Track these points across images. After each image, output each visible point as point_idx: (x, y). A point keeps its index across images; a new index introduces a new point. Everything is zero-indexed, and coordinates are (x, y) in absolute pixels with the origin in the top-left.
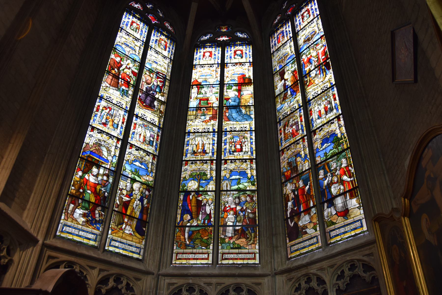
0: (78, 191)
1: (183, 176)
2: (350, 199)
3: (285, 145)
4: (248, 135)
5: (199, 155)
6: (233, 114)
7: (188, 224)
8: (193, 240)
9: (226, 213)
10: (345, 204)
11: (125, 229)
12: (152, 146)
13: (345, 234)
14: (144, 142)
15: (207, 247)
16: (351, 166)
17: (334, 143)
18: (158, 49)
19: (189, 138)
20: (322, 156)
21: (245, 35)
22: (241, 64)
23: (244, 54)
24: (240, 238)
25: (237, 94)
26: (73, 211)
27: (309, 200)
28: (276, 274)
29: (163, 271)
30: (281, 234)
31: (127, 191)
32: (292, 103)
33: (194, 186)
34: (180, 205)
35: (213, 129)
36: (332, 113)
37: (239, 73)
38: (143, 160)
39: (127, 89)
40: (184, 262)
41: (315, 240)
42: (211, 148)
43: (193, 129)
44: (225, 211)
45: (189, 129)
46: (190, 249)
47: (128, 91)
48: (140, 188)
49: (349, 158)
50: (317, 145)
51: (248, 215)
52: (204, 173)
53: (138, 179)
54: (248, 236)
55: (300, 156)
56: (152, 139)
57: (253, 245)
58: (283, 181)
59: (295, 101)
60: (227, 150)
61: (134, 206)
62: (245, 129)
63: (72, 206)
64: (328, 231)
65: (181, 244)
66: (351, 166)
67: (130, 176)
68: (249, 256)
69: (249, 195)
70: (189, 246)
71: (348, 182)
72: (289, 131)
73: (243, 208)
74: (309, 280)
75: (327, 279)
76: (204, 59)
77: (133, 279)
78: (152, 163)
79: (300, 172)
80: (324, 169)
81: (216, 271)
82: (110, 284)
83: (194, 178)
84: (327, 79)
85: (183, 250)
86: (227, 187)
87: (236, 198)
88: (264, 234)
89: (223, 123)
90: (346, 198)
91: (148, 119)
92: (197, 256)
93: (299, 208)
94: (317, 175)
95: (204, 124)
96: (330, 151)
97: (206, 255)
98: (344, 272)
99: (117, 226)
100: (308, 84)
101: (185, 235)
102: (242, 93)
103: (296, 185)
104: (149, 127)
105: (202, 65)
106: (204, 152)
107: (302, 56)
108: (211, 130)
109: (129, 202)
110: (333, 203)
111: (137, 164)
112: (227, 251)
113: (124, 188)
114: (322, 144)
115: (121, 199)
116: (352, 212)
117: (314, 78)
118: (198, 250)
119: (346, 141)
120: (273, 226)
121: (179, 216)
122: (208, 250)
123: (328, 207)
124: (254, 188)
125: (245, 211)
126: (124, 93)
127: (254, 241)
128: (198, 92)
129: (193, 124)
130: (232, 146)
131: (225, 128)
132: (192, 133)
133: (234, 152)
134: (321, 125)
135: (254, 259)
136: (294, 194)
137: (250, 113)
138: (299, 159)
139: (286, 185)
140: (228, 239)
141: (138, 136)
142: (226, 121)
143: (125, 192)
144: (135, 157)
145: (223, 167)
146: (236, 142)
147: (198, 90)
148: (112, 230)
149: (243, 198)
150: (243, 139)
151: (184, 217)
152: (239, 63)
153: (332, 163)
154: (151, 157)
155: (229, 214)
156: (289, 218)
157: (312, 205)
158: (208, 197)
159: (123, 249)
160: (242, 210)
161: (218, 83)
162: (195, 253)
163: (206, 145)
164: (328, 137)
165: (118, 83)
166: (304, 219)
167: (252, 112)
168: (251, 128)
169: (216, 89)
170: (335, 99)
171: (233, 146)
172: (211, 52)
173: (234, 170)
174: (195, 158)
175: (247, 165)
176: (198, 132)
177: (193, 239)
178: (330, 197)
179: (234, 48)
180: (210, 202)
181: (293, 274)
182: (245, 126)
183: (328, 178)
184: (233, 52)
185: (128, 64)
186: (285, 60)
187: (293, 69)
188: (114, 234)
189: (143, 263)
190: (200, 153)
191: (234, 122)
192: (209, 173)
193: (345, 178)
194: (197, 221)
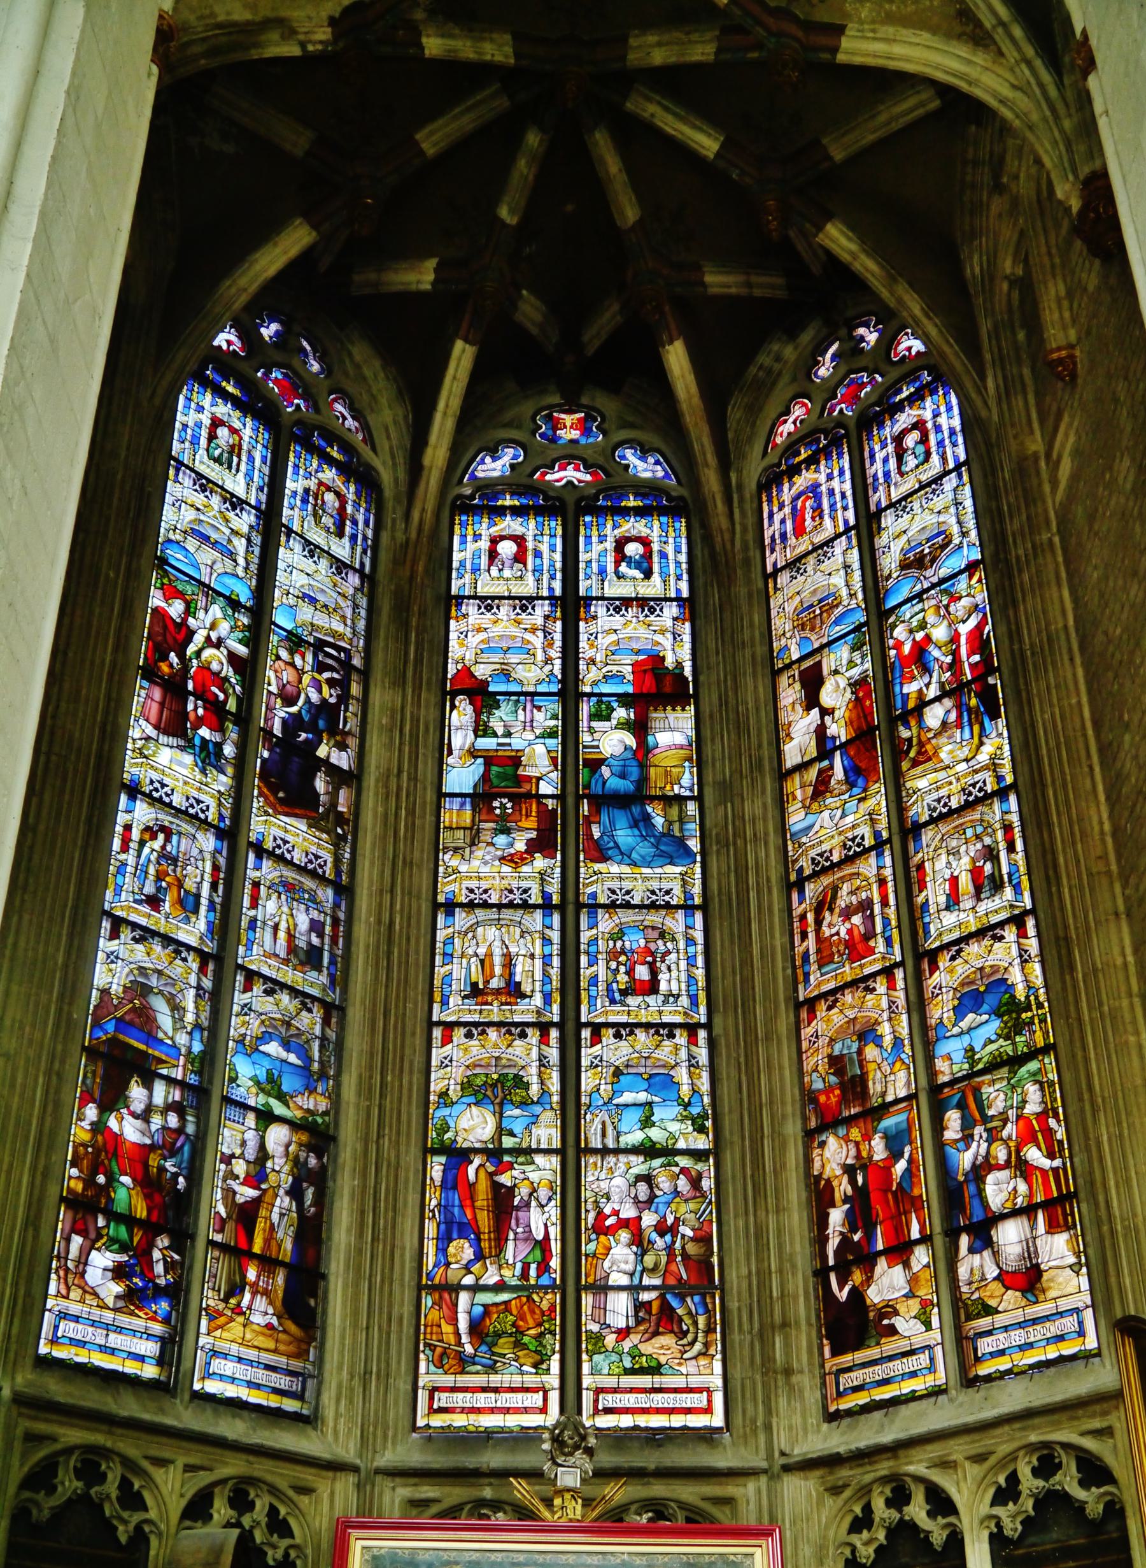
0: (89, 1182)
1: (436, 1087)
2: (1047, 1232)
3: (819, 985)
5: (495, 1003)
6: (619, 833)
7: (468, 1280)
8: (489, 1339)
9: (602, 1238)
10: (1030, 1251)
11: (250, 1308)
12: (318, 968)
13: (1027, 1353)
14: (291, 957)
16: (1056, 1116)
17: (1000, 1016)
18: (317, 536)
19: (451, 930)
20: (958, 1056)
21: (657, 463)
22: (642, 602)
23: (656, 558)
24: (656, 1334)
25: (631, 741)
26: (83, 1261)
27: (907, 1213)
28: (787, 1469)
29: (388, 1457)
30: (804, 1327)
31: (248, 1162)
32: (849, 819)
34: (434, 1202)
35: (543, 892)
36: (997, 898)
38: (293, 1031)
39: (216, 737)
40: (459, 1420)
41: (923, 1359)
42: (538, 975)
43: (464, 891)
44: (600, 1229)
45: (448, 889)
46: (477, 1373)
47: (219, 746)
48: (287, 1146)
49: (1051, 1084)
50: (941, 1010)
51: (683, 1248)
52: (516, 1076)
53: (279, 1109)
55: (878, 1041)
56: (315, 940)
57: (703, 1361)
58: (813, 1124)
59: (861, 812)
60: (602, 986)
61: (275, 1217)
62: (667, 898)
63: (77, 1241)
64: (971, 1333)
65: (444, 1354)
66: (1056, 1116)
67: (251, 1102)
68: (688, 1400)
69: (684, 1171)
70: (474, 1364)
71: (1043, 1172)
72: (838, 933)
74: (899, 1498)
75: (959, 1500)
76: (494, 571)
77: (291, 1493)
78: (323, 1039)
79: (876, 1102)
80: (962, 1106)
82: (216, 1516)
83: (480, 1096)
84: (983, 757)
85: (451, 1378)
86: (604, 1135)
87: (639, 1178)
89: (582, 870)
90: (1033, 1227)
91: (298, 857)
93: (870, 1237)
94: (938, 1126)
96: (985, 1046)
97: (535, 1396)
98: (1018, 1482)
99: (226, 1300)
100: (912, 754)
102: (650, 739)
103: (859, 1151)
104: (304, 891)
105: (486, 598)
106: (513, 991)
107: (893, 626)
108: (535, 898)
109: (256, 1203)
110: (991, 1238)
111: (273, 1048)
112: (611, 1382)
113: (238, 1152)
114: (959, 1012)
115: (230, 1193)
116: (1051, 1280)
117: (935, 736)
118: (507, 1378)
119: (1043, 1021)
120: (775, 1294)
121: (430, 1248)
122: (545, 1378)
123: (972, 1250)
124: (702, 1143)
125: (673, 1230)
126: (209, 756)
127: (706, 1345)
128: (477, 722)
129: (463, 868)
130: (617, 970)
131: (589, 890)
133: (624, 993)
134: (955, 935)
135: (708, 1410)
136: (853, 1181)
137: (681, 830)
138: (871, 1052)
139: (822, 1145)
140: (614, 1336)
141: (268, 932)
142: (592, 861)
143: (240, 1168)
144: (263, 1022)
147: (478, 713)
148: (211, 1319)
149: (664, 1182)
150: (660, 942)
151: (451, 1250)
152: (637, 599)
153: (991, 1090)
154: (318, 1013)
155: (613, 1244)
156: (832, 1268)
157: (915, 1234)
158: (534, 1176)
159: (251, 1385)
160: (662, 1229)
161: (554, 688)
162: (496, 1390)
163: (521, 958)
164: (982, 989)
165: (185, 715)
166: (885, 1280)
167: (692, 826)
168: (688, 896)
169: (546, 717)
170: (1011, 848)
171: (622, 969)
172: (520, 540)
173: (627, 1066)
174: (481, 1012)
175: (677, 1048)
176: (485, 905)
177: (487, 1335)
178: (978, 1215)
179: (614, 527)
180: (543, 1194)
181: (844, 1473)
182: (666, 886)
183: (975, 1144)
184: (610, 544)
185: (213, 627)
186: (822, 623)
187: (855, 672)
188: (218, 1333)
189: (315, 1429)
190: (497, 992)
191: (626, 869)
192: (535, 1079)
193: (1034, 1155)
194: (500, 1267)
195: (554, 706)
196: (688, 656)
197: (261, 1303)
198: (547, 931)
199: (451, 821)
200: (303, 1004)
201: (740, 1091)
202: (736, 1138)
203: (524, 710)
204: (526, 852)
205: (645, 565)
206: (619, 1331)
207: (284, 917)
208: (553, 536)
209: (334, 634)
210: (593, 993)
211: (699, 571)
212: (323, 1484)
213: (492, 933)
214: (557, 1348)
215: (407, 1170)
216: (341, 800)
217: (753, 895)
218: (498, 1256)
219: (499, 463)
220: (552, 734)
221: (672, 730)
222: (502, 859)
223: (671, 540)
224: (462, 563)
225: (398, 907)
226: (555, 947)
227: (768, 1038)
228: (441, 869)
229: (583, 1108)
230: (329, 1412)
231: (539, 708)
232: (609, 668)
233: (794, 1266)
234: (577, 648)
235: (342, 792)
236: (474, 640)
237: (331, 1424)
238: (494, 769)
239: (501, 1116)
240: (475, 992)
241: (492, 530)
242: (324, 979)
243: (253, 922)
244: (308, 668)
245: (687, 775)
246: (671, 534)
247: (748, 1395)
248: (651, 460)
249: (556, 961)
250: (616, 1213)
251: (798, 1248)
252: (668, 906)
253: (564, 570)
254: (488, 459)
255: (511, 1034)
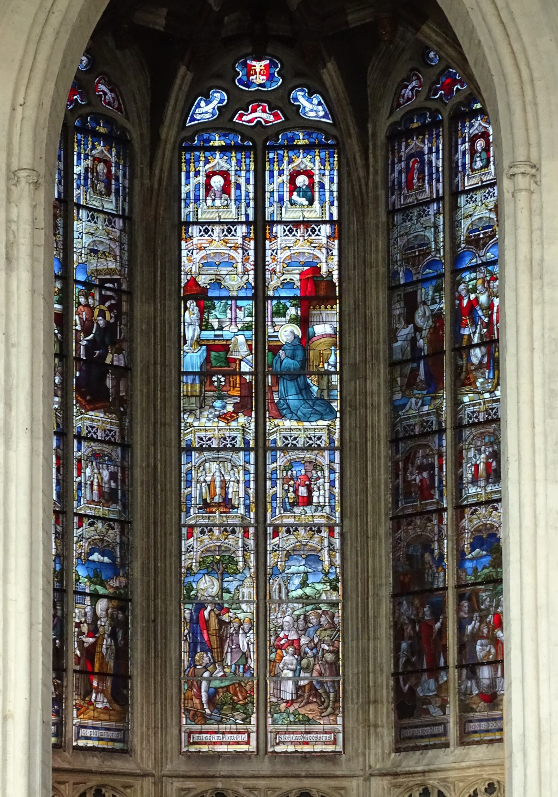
3: (403, 509)
4: (324, 459)
5: (217, 512)
6: (290, 397)
9: (279, 651)
11: (95, 701)
14: (101, 500)
15: (246, 720)
18: (95, 203)
19: (190, 465)
21: (320, 104)
22: (307, 224)
23: (316, 189)
24: (308, 703)
25: (298, 332)
28: (371, 775)
29: (168, 768)
30: (385, 703)
31: (88, 624)
33: (210, 590)
34: (186, 631)
35: (244, 439)
37: (302, 260)
38: (105, 544)
40: (205, 748)
42: (242, 494)
43: (197, 439)
45: (188, 437)
46: (213, 724)
52: (230, 557)
53: (101, 591)
54: (323, 700)
56: (113, 484)
61: (104, 650)
62: (318, 442)
65: (195, 714)
67: (87, 591)
70: (211, 719)
73: (312, 640)
77: (122, 789)
81: (265, 767)
83: (210, 570)
85: (199, 727)
86: (280, 592)
87: (298, 617)
88: (352, 699)
89: (268, 424)
91: (100, 435)
92: (229, 737)
95: (222, 424)
97: (243, 736)
99: (84, 699)
101: (201, 696)
102: (310, 329)
105: (205, 223)
108: (239, 444)
109: (94, 645)
111: (96, 557)
113: (83, 620)
115: (81, 643)
118: (228, 726)
121: (185, 657)
122: (248, 726)
124: (334, 596)
127: (334, 709)
128: (201, 319)
129: (196, 424)
131: (272, 438)
132: (195, 449)
133: (293, 505)
137: (329, 395)
142: (273, 418)
143: (85, 628)
144: (89, 543)
145: (272, 543)
146: (297, 477)
147: (201, 312)
148: (78, 710)
150: (314, 472)
151: (197, 658)
152: (303, 222)
155: (285, 654)
158: (241, 616)
159: (99, 739)
163: (232, 483)
167: (335, 393)
168: (332, 441)
171: (291, 489)
172: (225, 174)
173: (294, 550)
174: (209, 518)
175: (322, 539)
180: (246, 626)
182: (318, 433)
184: (285, 177)
188: (82, 716)
189: (131, 756)
190: (218, 505)
191: (294, 423)
192: (241, 559)
194: (224, 667)
195: (249, 304)
196: (336, 267)
197: (100, 697)
198: (247, 466)
199: (187, 391)
200: (109, 525)
201: (357, 568)
202: (354, 595)
203: (231, 310)
204: (234, 412)
205: (309, 193)
206: (287, 702)
207: (96, 475)
208: (248, 171)
209: (110, 271)
210: (274, 505)
211: (345, 200)
212: (137, 783)
213: (214, 466)
214: (255, 710)
215: (171, 614)
216: (122, 388)
217: (369, 444)
218: (222, 661)
219: (211, 106)
220: (248, 328)
221: (324, 323)
222: (219, 417)
223: (327, 173)
224: (188, 194)
225: (159, 457)
226: (252, 475)
227: (374, 538)
228: (183, 425)
229: (268, 576)
230: (138, 749)
231: (240, 308)
232: (285, 277)
233: (382, 670)
234: (264, 261)
235: (121, 383)
236: (198, 256)
237: (139, 753)
238: (213, 353)
239: (222, 580)
240: (206, 505)
241: (208, 166)
242: (119, 508)
243: (80, 484)
244: (97, 303)
245: (333, 357)
246: (328, 167)
247: (355, 736)
248: (315, 101)
249: (252, 485)
250: (286, 637)
251: (384, 660)
252: (319, 448)
253: (255, 199)
254: (203, 104)
255: (227, 532)
